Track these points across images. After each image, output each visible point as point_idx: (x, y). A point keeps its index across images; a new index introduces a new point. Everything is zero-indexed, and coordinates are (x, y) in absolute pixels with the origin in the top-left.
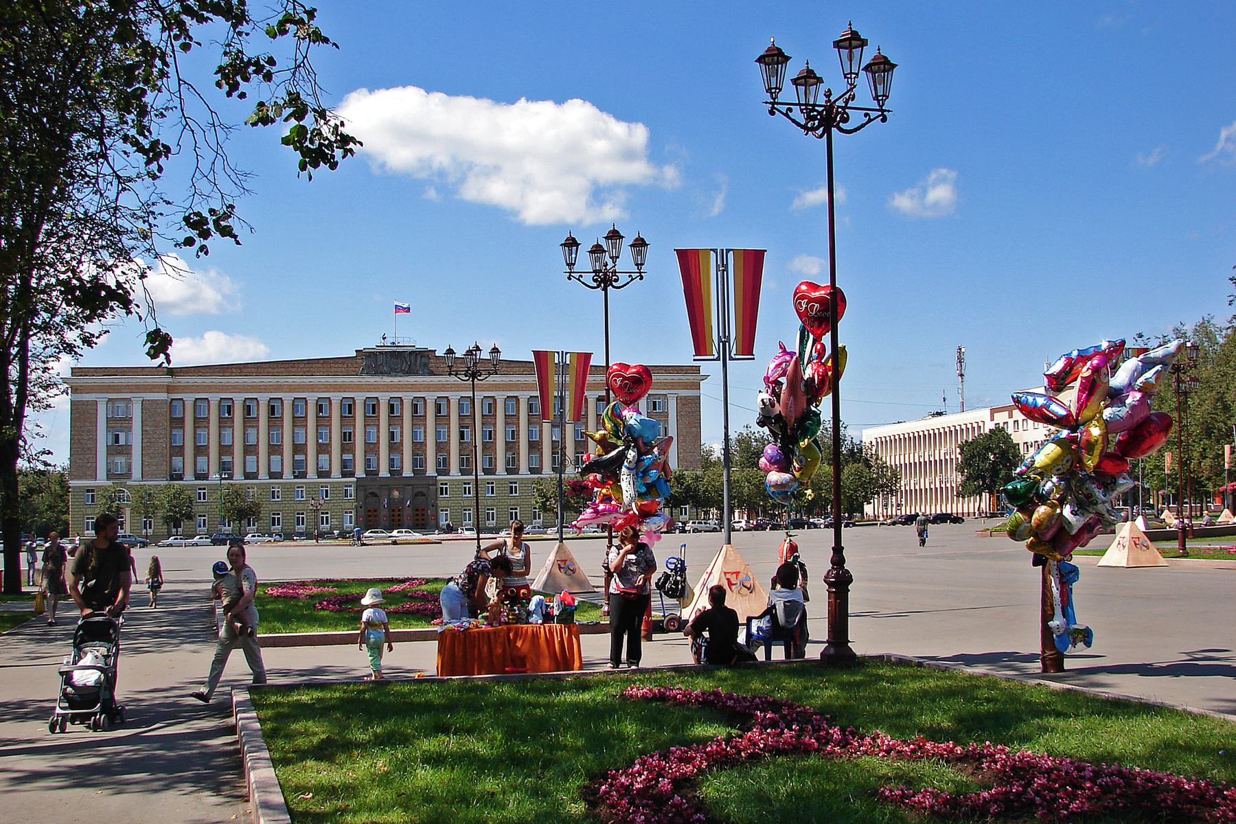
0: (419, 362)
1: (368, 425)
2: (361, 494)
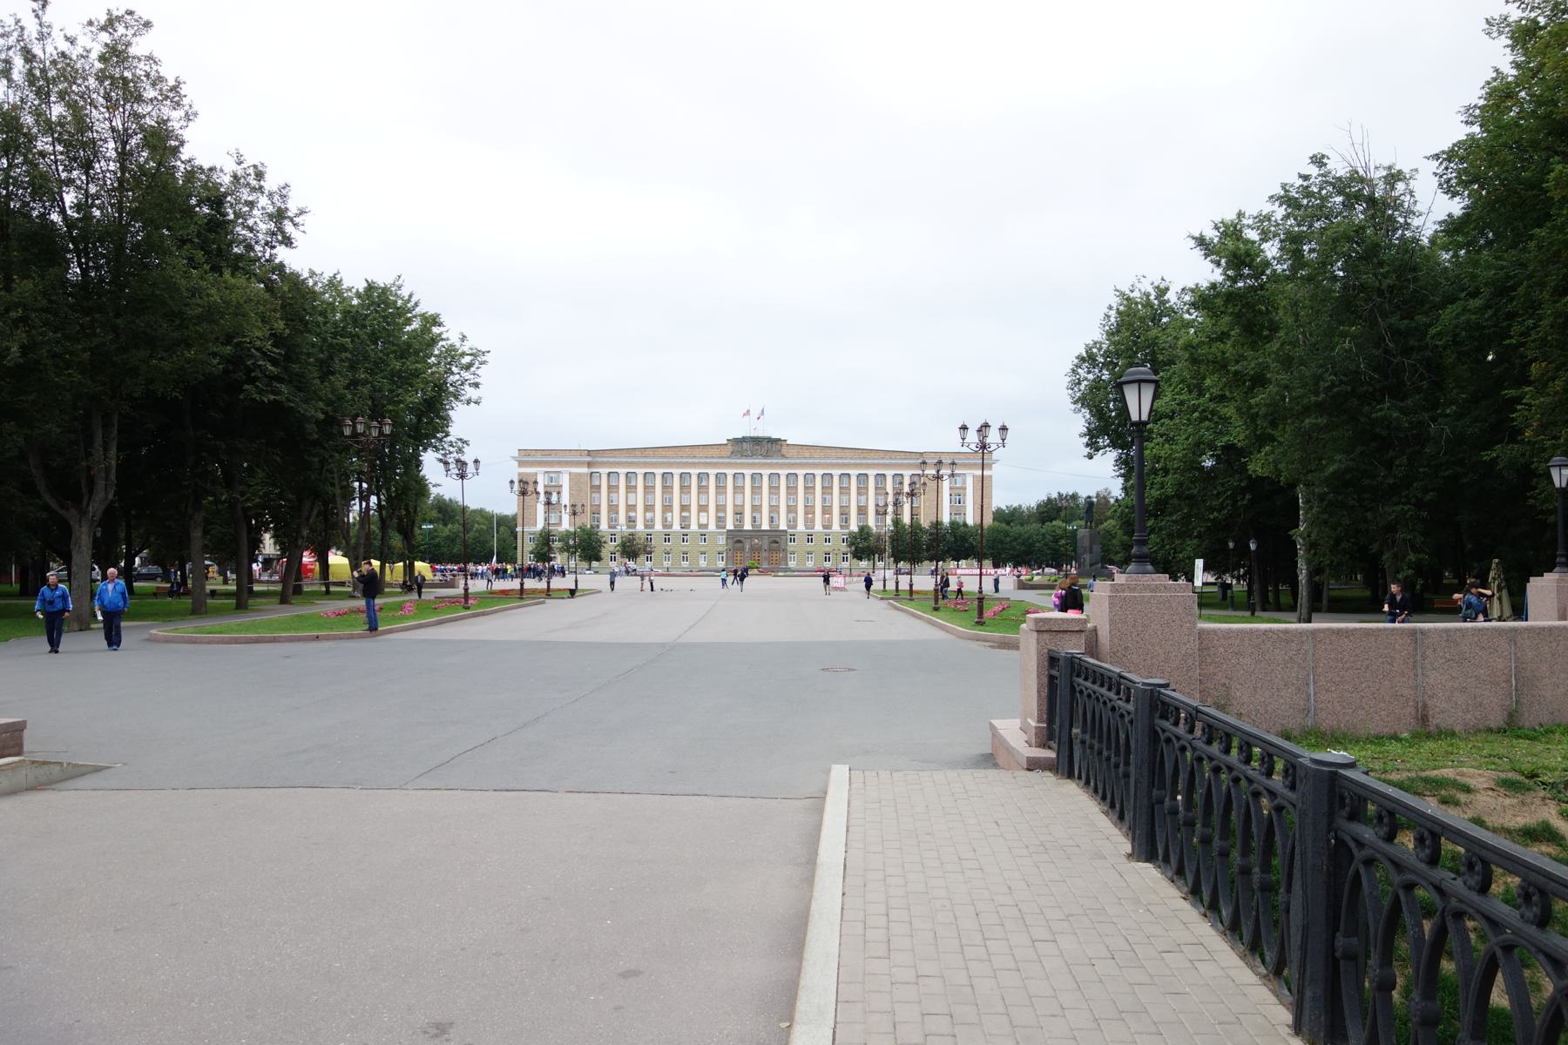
2: (730, 541)
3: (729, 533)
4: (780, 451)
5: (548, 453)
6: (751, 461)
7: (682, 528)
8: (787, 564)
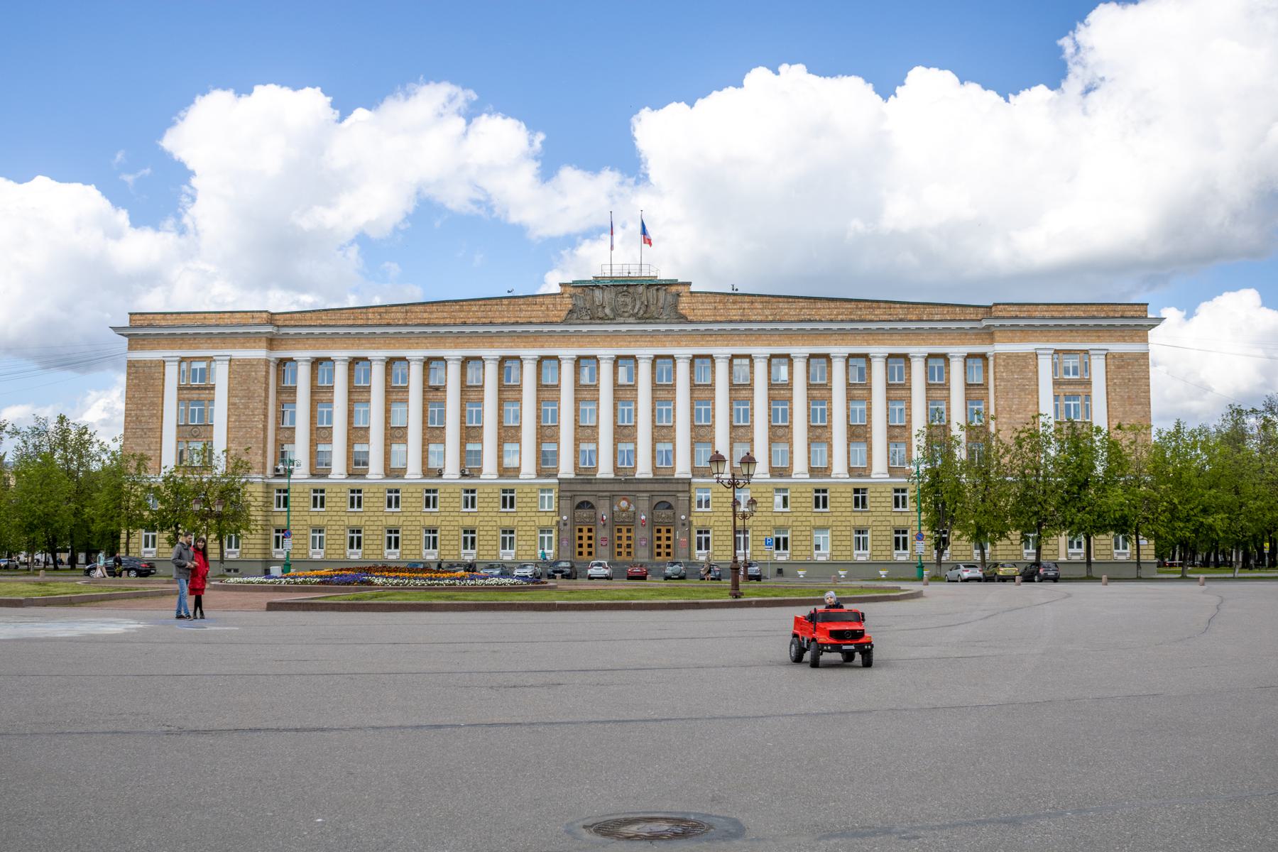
1: (584, 400)
3: (564, 487)
4: (675, 306)
6: (611, 328)
7: (463, 475)
8: (690, 555)
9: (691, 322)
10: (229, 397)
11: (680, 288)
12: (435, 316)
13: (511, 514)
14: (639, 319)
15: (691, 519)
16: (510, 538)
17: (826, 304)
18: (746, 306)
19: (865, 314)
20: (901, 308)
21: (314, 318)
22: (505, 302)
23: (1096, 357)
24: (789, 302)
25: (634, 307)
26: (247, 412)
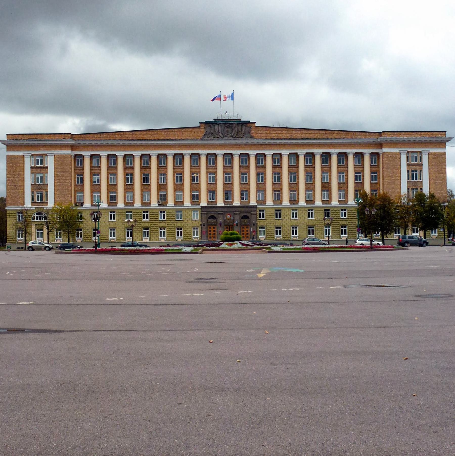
0: (244, 130)
3: (203, 210)
4: (249, 132)
5: (34, 137)
7: (159, 205)
9: (256, 139)
10: (54, 172)
11: (251, 125)
12: (145, 136)
13: (280, 220)
14: (234, 138)
15: (257, 222)
16: (279, 230)
17: (313, 132)
18: (279, 132)
19: (329, 135)
20: (344, 133)
21: (91, 136)
22: (176, 130)
23: (424, 154)
24: (297, 131)
25: (232, 133)
26: (63, 178)
